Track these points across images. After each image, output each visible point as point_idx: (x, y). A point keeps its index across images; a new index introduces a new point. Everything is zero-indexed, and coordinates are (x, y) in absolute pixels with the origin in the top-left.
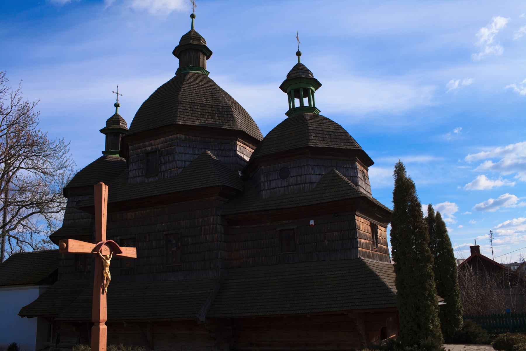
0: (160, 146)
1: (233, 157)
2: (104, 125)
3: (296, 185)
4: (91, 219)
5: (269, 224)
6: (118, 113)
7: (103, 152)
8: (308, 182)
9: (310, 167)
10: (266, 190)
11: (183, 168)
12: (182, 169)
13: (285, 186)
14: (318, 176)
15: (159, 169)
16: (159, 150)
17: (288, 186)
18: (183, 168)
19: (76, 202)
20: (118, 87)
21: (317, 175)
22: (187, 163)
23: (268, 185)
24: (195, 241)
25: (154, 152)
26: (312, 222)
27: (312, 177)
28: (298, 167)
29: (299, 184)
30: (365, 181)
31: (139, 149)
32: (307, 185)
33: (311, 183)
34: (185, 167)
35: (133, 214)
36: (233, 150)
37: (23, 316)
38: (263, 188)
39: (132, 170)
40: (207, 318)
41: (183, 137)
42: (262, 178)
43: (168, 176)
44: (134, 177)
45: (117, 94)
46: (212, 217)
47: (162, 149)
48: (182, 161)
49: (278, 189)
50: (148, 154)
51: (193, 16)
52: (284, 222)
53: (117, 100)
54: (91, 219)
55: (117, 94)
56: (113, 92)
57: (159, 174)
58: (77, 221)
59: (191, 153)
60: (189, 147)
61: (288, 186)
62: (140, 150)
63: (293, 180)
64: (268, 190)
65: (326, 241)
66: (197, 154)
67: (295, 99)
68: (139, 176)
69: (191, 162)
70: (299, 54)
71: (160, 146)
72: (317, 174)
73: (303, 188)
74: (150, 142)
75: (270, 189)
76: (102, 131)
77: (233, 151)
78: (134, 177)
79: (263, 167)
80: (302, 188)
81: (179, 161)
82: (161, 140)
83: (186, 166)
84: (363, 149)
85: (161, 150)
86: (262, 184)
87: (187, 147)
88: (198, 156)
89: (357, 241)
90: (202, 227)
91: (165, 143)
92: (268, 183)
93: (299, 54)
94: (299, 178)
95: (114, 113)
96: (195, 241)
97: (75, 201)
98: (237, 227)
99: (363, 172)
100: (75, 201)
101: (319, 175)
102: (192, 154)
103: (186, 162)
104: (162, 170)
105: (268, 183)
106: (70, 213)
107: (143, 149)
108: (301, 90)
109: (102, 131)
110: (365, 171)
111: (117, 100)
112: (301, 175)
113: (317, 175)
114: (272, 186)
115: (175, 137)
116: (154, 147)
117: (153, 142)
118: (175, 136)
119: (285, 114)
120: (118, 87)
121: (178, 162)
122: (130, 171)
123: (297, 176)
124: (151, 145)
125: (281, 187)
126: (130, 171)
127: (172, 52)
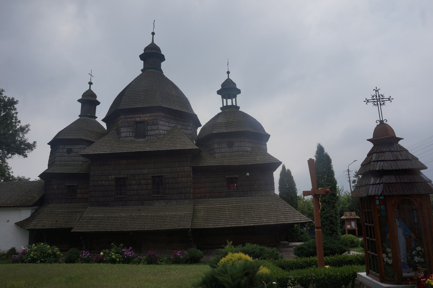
0: (146, 119)
1: (190, 130)
2: (80, 97)
3: (238, 152)
5: (221, 173)
6: (92, 89)
8: (245, 151)
9: (246, 142)
10: (218, 153)
11: (164, 135)
12: (163, 135)
13: (230, 152)
14: (250, 148)
15: (147, 134)
16: (146, 121)
17: (233, 152)
18: (164, 135)
19: (66, 149)
21: (250, 147)
23: (220, 150)
24: (174, 182)
25: (143, 122)
26: (248, 174)
27: (248, 148)
28: (239, 141)
31: (130, 119)
32: (245, 152)
33: (247, 151)
34: (164, 134)
36: (190, 126)
39: (124, 132)
41: (163, 114)
42: (216, 146)
44: (126, 137)
45: (91, 75)
46: (187, 167)
47: (148, 121)
48: (163, 130)
49: (226, 153)
50: (137, 123)
51: (153, 34)
53: (91, 80)
55: (91, 75)
57: (146, 137)
59: (168, 125)
60: (167, 122)
61: (233, 152)
62: (130, 119)
64: (220, 153)
65: (256, 185)
66: (171, 127)
69: (168, 131)
70: (228, 73)
71: (146, 119)
72: (250, 146)
73: (242, 154)
74: (139, 115)
75: (221, 153)
76: (79, 101)
77: (190, 127)
78: (126, 137)
79: (216, 139)
80: (241, 154)
81: (161, 130)
82: (148, 115)
83: (165, 133)
85: (148, 121)
86: (216, 149)
87: (165, 121)
88: (172, 128)
90: (180, 173)
91: (151, 117)
92: (219, 149)
93: (228, 73)
94: (240, 148)
95: (88, 88)
96: (174, 182)
97: (66, 148)
100: (66, 148)
101: (250, 147)
102: (168, 126)
103: (165, 131)
104: (149, 135)
105: (219, 149)
106: (61, 157)
109: (79, 101)
111: (91, 80)
113: (250, 147)
114: (222, 151)
115: (159, 114)
117: (141, 115)
118: (159, 114)
121: (161, 130)
122: (122, 132)
123: (238, 147)
124: (140, 117)
125: (228, 152)
126: (122, 132)
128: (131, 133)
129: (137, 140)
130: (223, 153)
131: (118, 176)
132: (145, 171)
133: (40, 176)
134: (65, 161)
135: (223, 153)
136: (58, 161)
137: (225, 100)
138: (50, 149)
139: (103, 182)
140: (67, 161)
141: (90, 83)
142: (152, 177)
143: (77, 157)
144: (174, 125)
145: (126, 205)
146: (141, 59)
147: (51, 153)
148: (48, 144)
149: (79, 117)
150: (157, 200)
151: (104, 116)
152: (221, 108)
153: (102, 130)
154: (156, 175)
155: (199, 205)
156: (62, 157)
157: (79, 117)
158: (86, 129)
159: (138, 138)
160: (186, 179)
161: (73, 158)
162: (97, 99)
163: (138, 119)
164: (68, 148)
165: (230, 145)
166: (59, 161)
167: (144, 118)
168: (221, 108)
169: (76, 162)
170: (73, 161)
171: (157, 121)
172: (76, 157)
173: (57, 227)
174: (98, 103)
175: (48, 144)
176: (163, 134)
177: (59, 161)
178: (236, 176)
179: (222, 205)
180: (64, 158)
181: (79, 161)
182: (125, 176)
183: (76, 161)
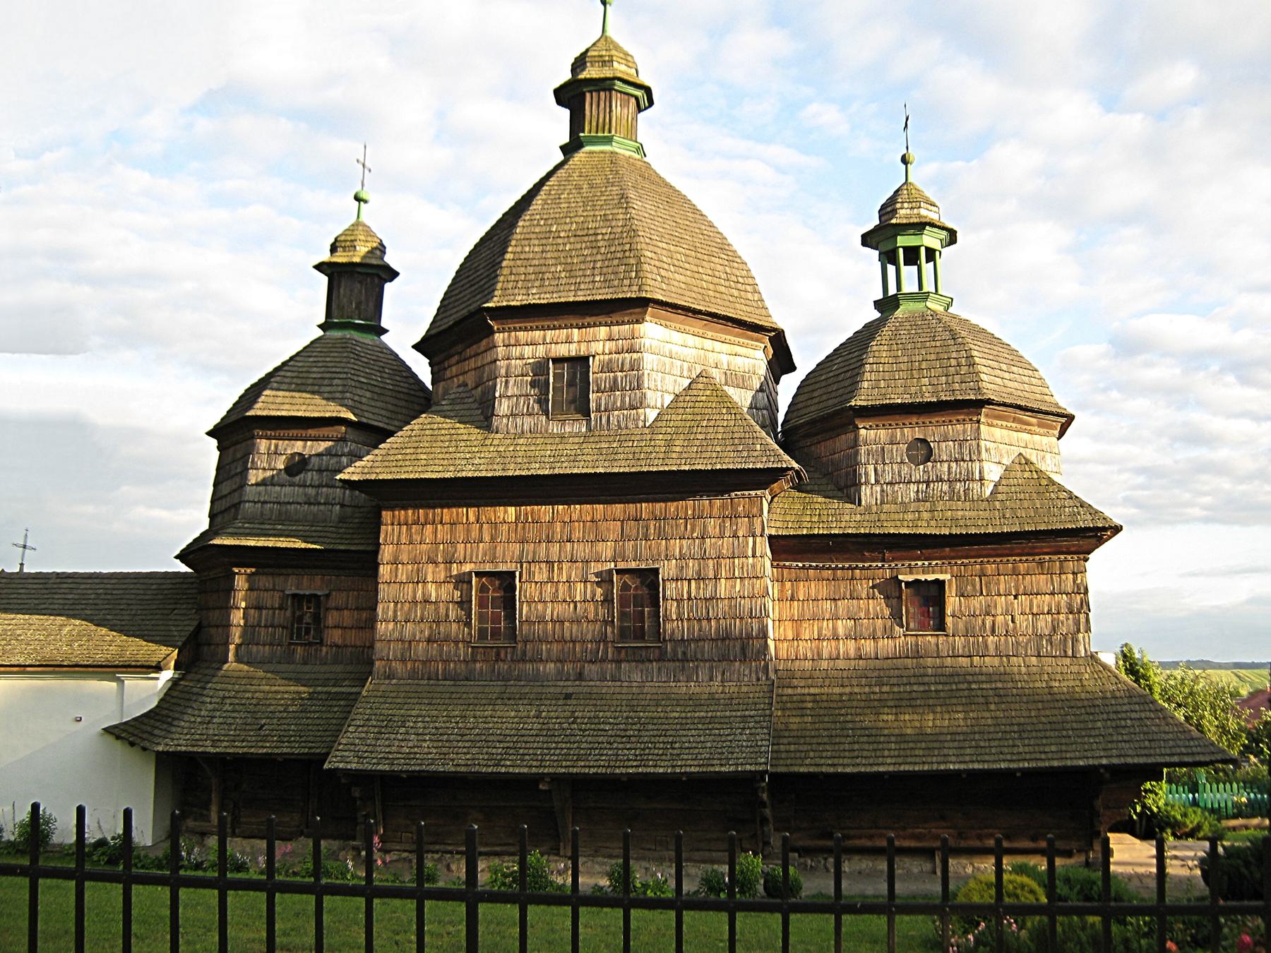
4: (338, 506)
20: (365, 147)
35: (511, 510)
43: (620, 427)
54: (338, 506)
55: (364, 165)
56: (358, 161)
76: (320, 267)
95: (353, 220)
101: (999, 463)
108: (923, 251)
109: (320, 267)
119: (875, 302)
120: (365, 147)
127: (557, 85)
129: (555, 428)
133: (182, 557)
134: (279, 503)
136: (255, 502)
137: (891, 269)
138: (215, 455)
140: (289, 503)
143: (325, 490)
146: (560, 102)
147: (219, 468)
148: (210, 434)
151: (418, 334)
152: (878, 304)
153: (412, 381)
156: (269, 488)
157: (321, 333)
158: (356, 378)
161: (311, 491)
162: (386, 259)
164: (289, 452)
166: (259, 502)
167: (583, 347)
168: (878, 304)
169: (322, 507)
170: (310, 504)
171: (635, 356)
172: (323, 486)
173: (265, 751)
174: (393, 274)
175: (210, 434)
177: (259, 502)
178: (941, 577)
179: (885, 689)
180: (278, 488)
181: (333, 505)
183: (319, 504)
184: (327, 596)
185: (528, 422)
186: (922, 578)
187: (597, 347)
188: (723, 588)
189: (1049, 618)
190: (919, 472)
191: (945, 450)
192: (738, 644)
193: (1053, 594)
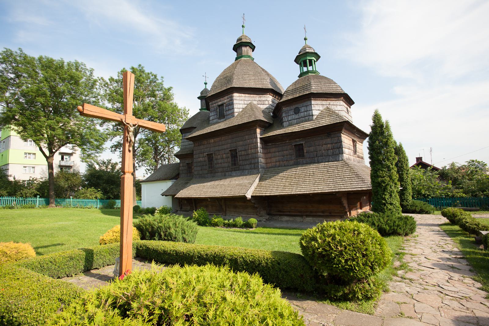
2: (199, 95)
3: (304, 117)
7: (200, 110)
13: (297, 119)
16: (225, 103)
17: (299, 118)
22: (241, 110)
25: (222, 105)
29: (306, 117)
30: (348, 114)
37: (163, 195)
38: (284, 120)
40: (252, 196)
42: (284, 115)
44: (213, 120)
50: (219, 106)
52: (297, 140)
53: (206, 81)
58: (187, 146)
61: (299, 118)
63: (302, 114)
64: (287, 121)
67: (304, 68)
68: (215, 119)
76: (199, 98)
78: (213, 120)
79: (284, 108)
82: (226, 97)
84: (346, 92)
86: (284, 118)
89: (342, 150)
93: (305, 39)
94: (305, 113)
95: (204, 88)
98: (269, 144)
99: (347, 108)
107: (217, 104)
108: (308, 60)
109: (199, 98)
110: (348, 108)
111: (206, 81)
112: (307, 111)
114: (290, 119)
116: (222, 102)
117: (222, 99)
125: (295, 119)
128: (216, 116)
129: (219, 121)
130: (290, 120)
131: (209, 153)
132: (225, 147)
135: (290, 120)
139: (201, 159)
141: (206, 84)
142: (230, 151)
144: (250, 102)
145: (215, 177)
149: (199, 111)
150: (235, 171)
154: (233, 149)
155: (268, 173)
159: (220, 119)
160: (254, 150)
163: (220, 103)
165: (297, 111)
176: (238, 111)
178: (302, 143)
182: (213, 152)
184: (192, 163)
185: (215, 121)
186: (297, 144)
187: (225, 101)
188: (250, 151)
189: (331, 151)
190: (297, 116)
191: (302, 109)
192: (253, 165)
193: (332, 144)
